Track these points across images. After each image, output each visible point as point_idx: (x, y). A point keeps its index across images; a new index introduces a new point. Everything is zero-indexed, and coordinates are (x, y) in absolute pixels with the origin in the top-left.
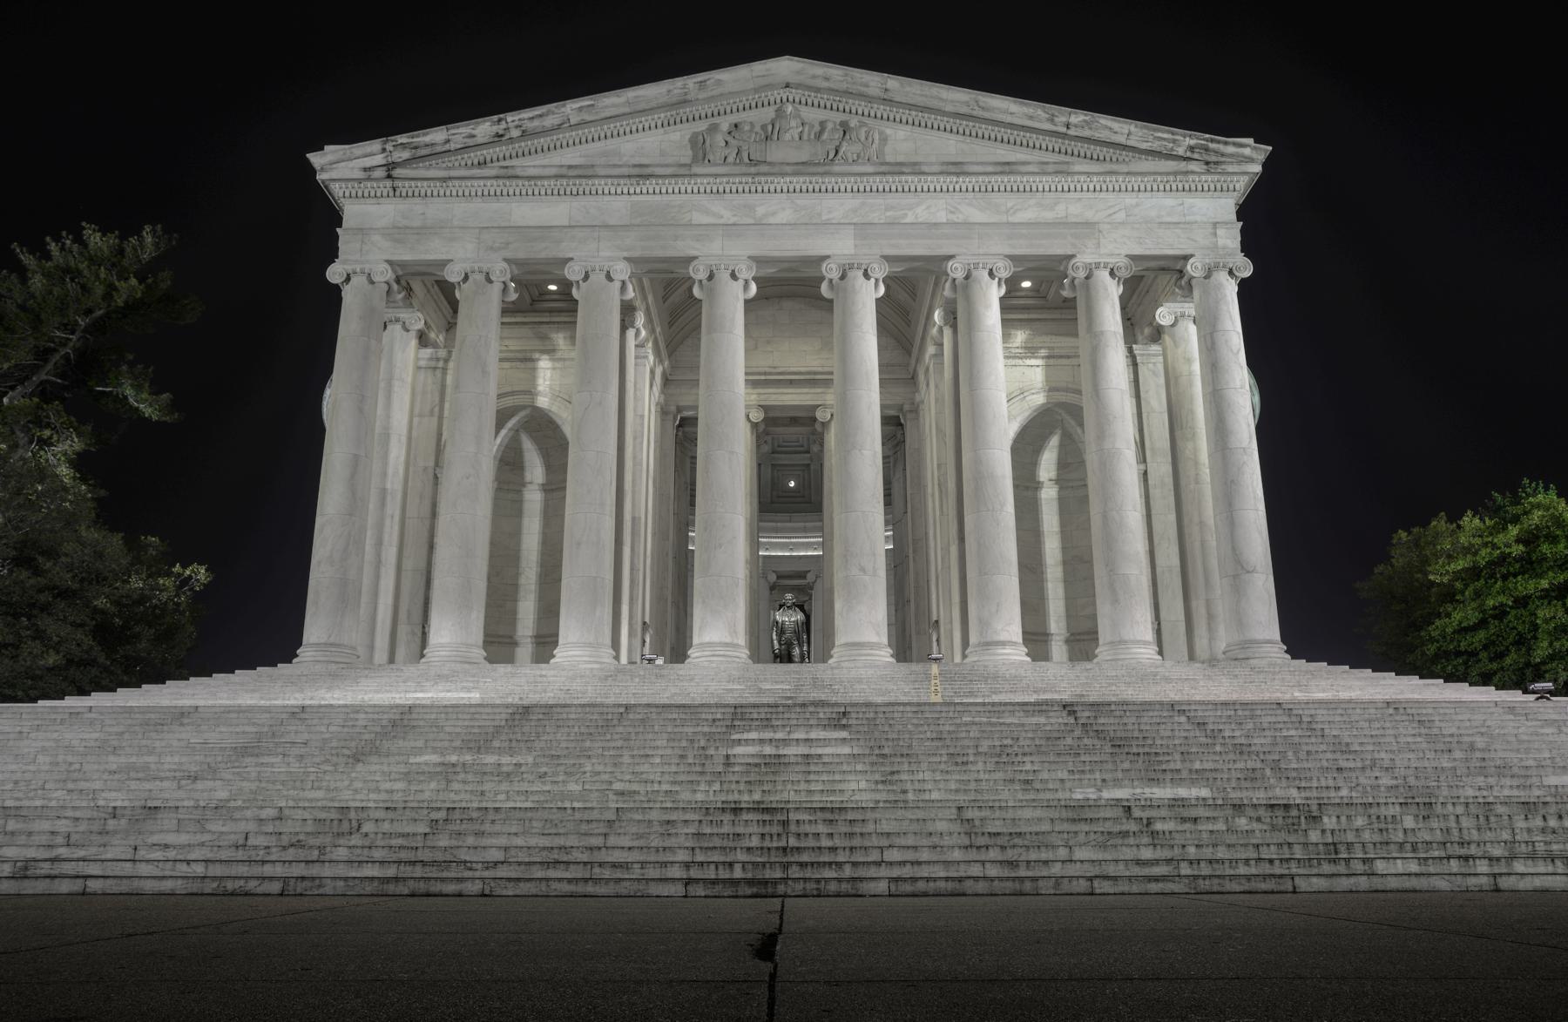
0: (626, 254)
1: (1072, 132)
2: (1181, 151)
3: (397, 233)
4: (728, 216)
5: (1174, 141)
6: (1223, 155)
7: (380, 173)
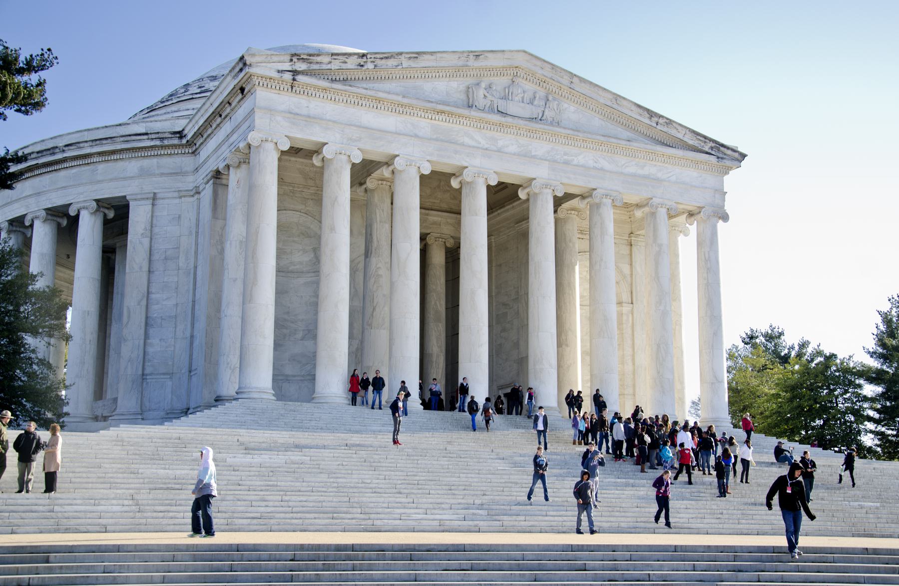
0: (429, 158)
2: (707, 149)
3: (293, 115)
4: (484, 143)
7: (288, 76)
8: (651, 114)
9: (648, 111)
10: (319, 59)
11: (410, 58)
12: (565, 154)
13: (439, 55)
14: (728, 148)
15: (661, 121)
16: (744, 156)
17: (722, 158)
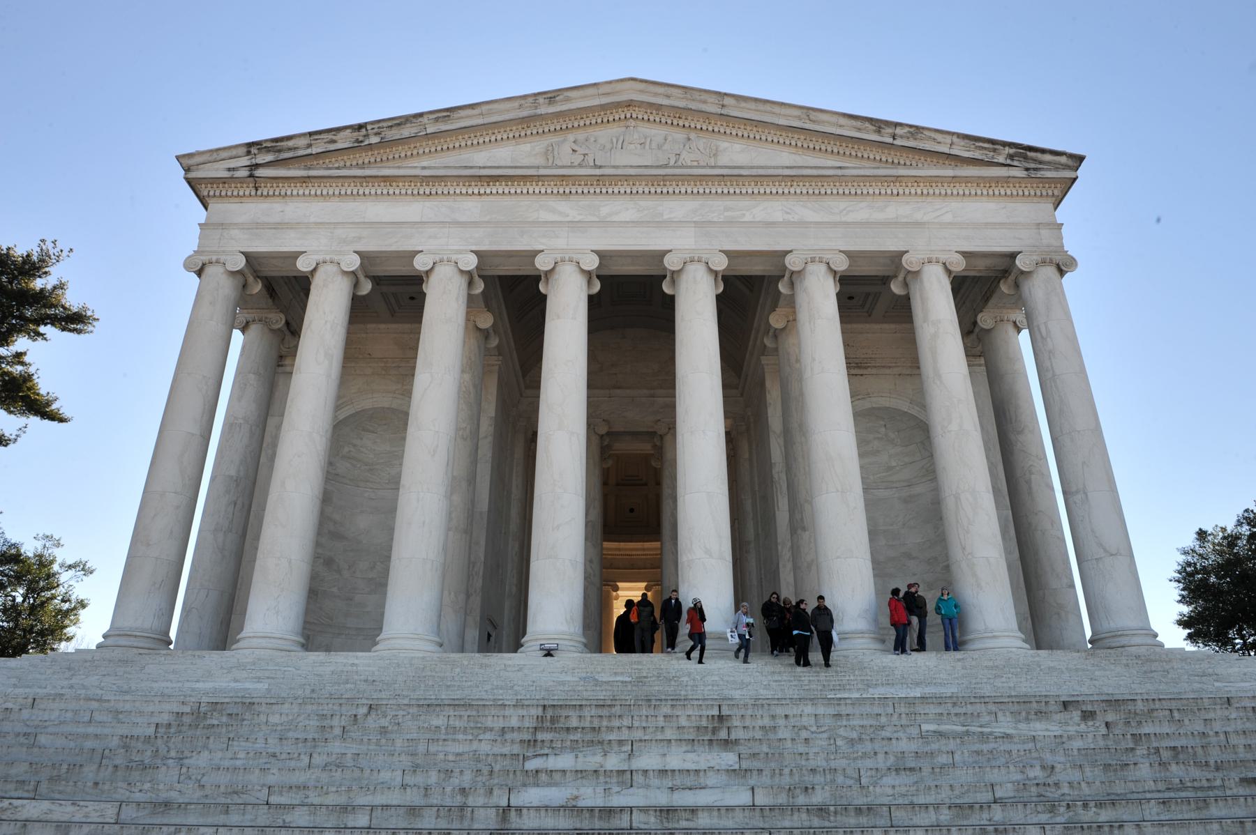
0: (474, 248)
1: (898, 142)
2: (1001, 159)
3: (256, 227)
5: (995, 150)
6: (1041, 163)
8: (879, 125)
9: (870, 120)
10: (290, 143)
11: (437, 120)
12: (727, 209)
13: (485, 108)
14: (1043, 151)
15: (899, 131)
16: (1081, 159)
17: (1035, 169)
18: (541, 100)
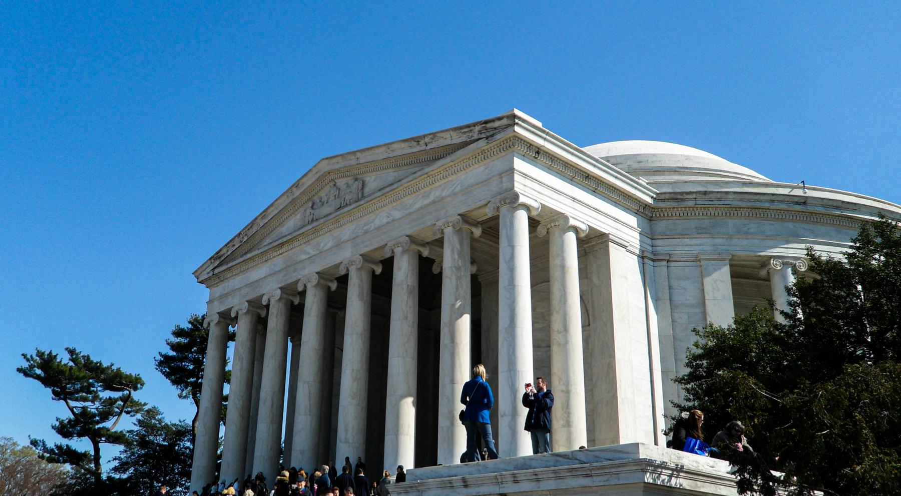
1: (429, 147)
6: (495, 128)
8: (417, 140)
9: (412, 139)
10: (222, 253)
14: (493, 121)
15: (427, 140)
17: (492, 136)
18: (294, 190)
